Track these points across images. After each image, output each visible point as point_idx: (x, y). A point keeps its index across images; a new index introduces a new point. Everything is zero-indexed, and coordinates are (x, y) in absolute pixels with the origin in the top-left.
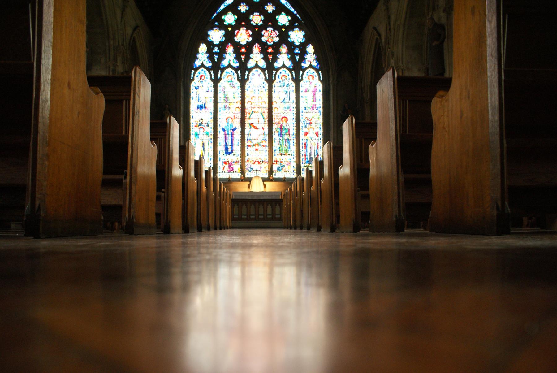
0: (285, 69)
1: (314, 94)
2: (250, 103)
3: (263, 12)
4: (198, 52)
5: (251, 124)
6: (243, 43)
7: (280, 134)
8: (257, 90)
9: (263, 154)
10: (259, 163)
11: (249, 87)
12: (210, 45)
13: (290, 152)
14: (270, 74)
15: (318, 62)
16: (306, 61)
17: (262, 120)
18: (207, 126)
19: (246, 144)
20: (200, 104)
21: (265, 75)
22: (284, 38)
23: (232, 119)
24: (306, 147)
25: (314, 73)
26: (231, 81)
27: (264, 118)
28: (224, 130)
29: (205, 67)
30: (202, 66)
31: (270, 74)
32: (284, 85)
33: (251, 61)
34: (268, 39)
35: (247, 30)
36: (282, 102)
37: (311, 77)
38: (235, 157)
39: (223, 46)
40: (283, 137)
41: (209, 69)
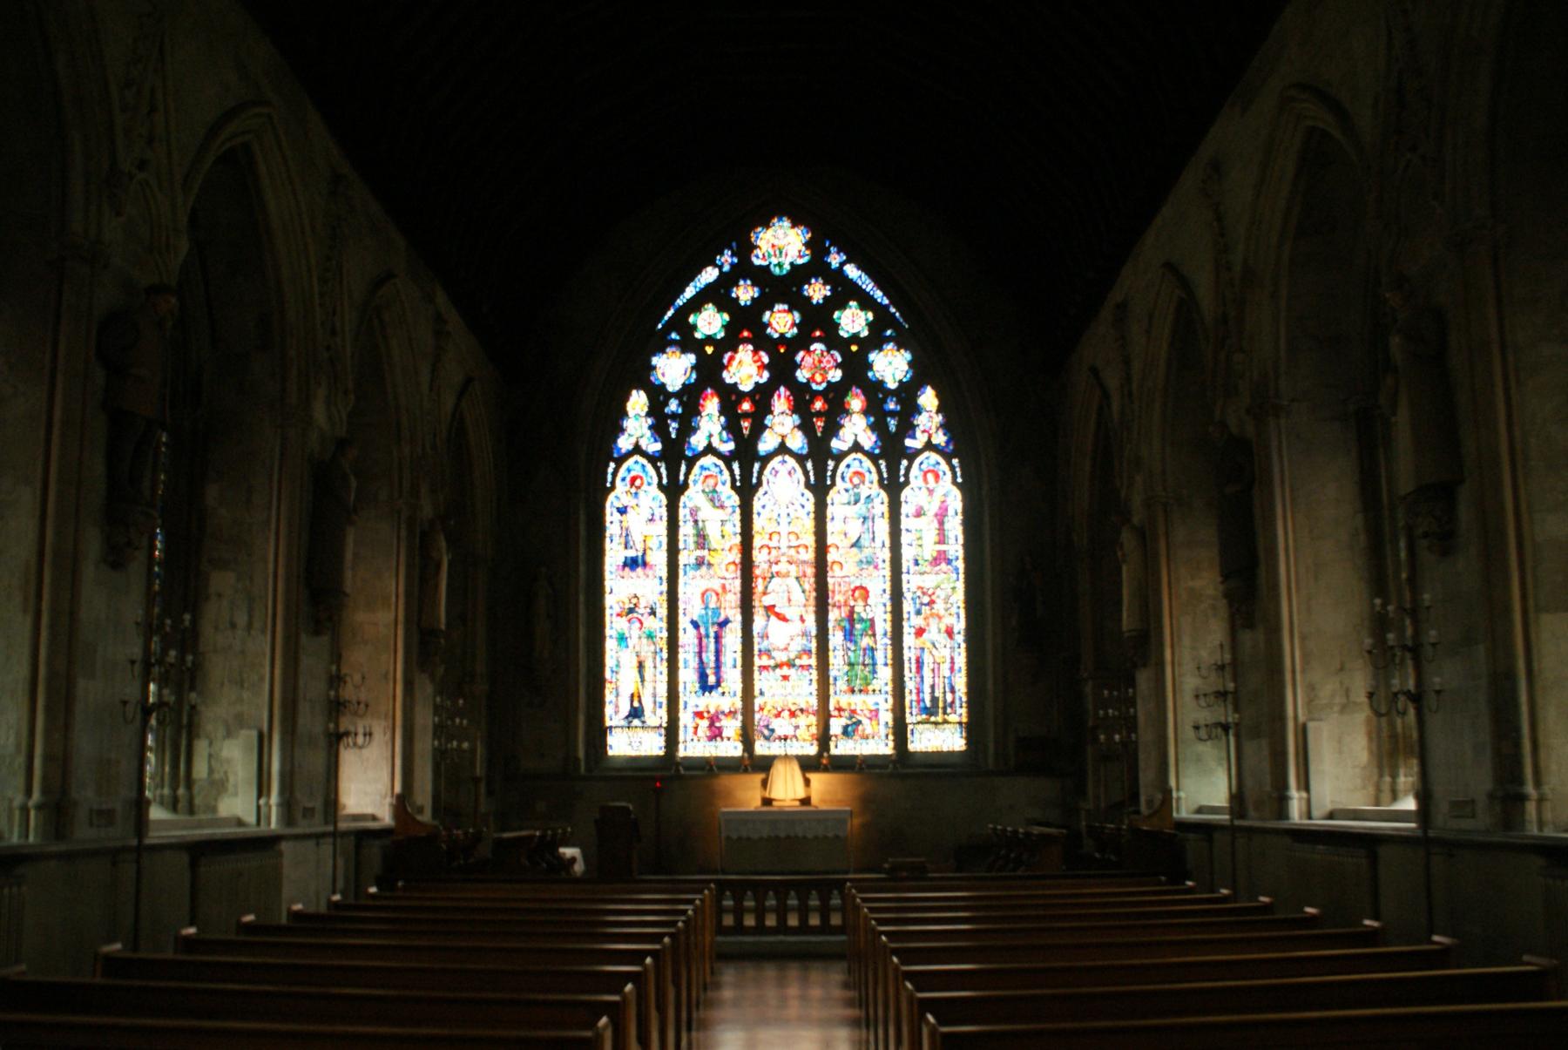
0: (860, 456)
2: (765, 551)
4: (625, 414)
6: (746, 387)
7: (849, 635)
11: (764, 507)
12: (658, 395)
13: (876, 684)
14: (820, 470)
15: (948, 435)
16: (918, 433)
17: (798, 597)
19: (757, 662)
20: (631, 553)
21: (806, 473)
23: (717, 594)
25: (938, 463)
26: (714, 491)
27: (804, 592)
28: (695, 625)
29: (644, 454)
30: (637, 450)
31: (820, 470)
33: (767, 434)
34: (813, 375)
36: (852, 546)
37: (930, 477)
38: (728, 698)
39: (691, 397)
41: (653, 459)
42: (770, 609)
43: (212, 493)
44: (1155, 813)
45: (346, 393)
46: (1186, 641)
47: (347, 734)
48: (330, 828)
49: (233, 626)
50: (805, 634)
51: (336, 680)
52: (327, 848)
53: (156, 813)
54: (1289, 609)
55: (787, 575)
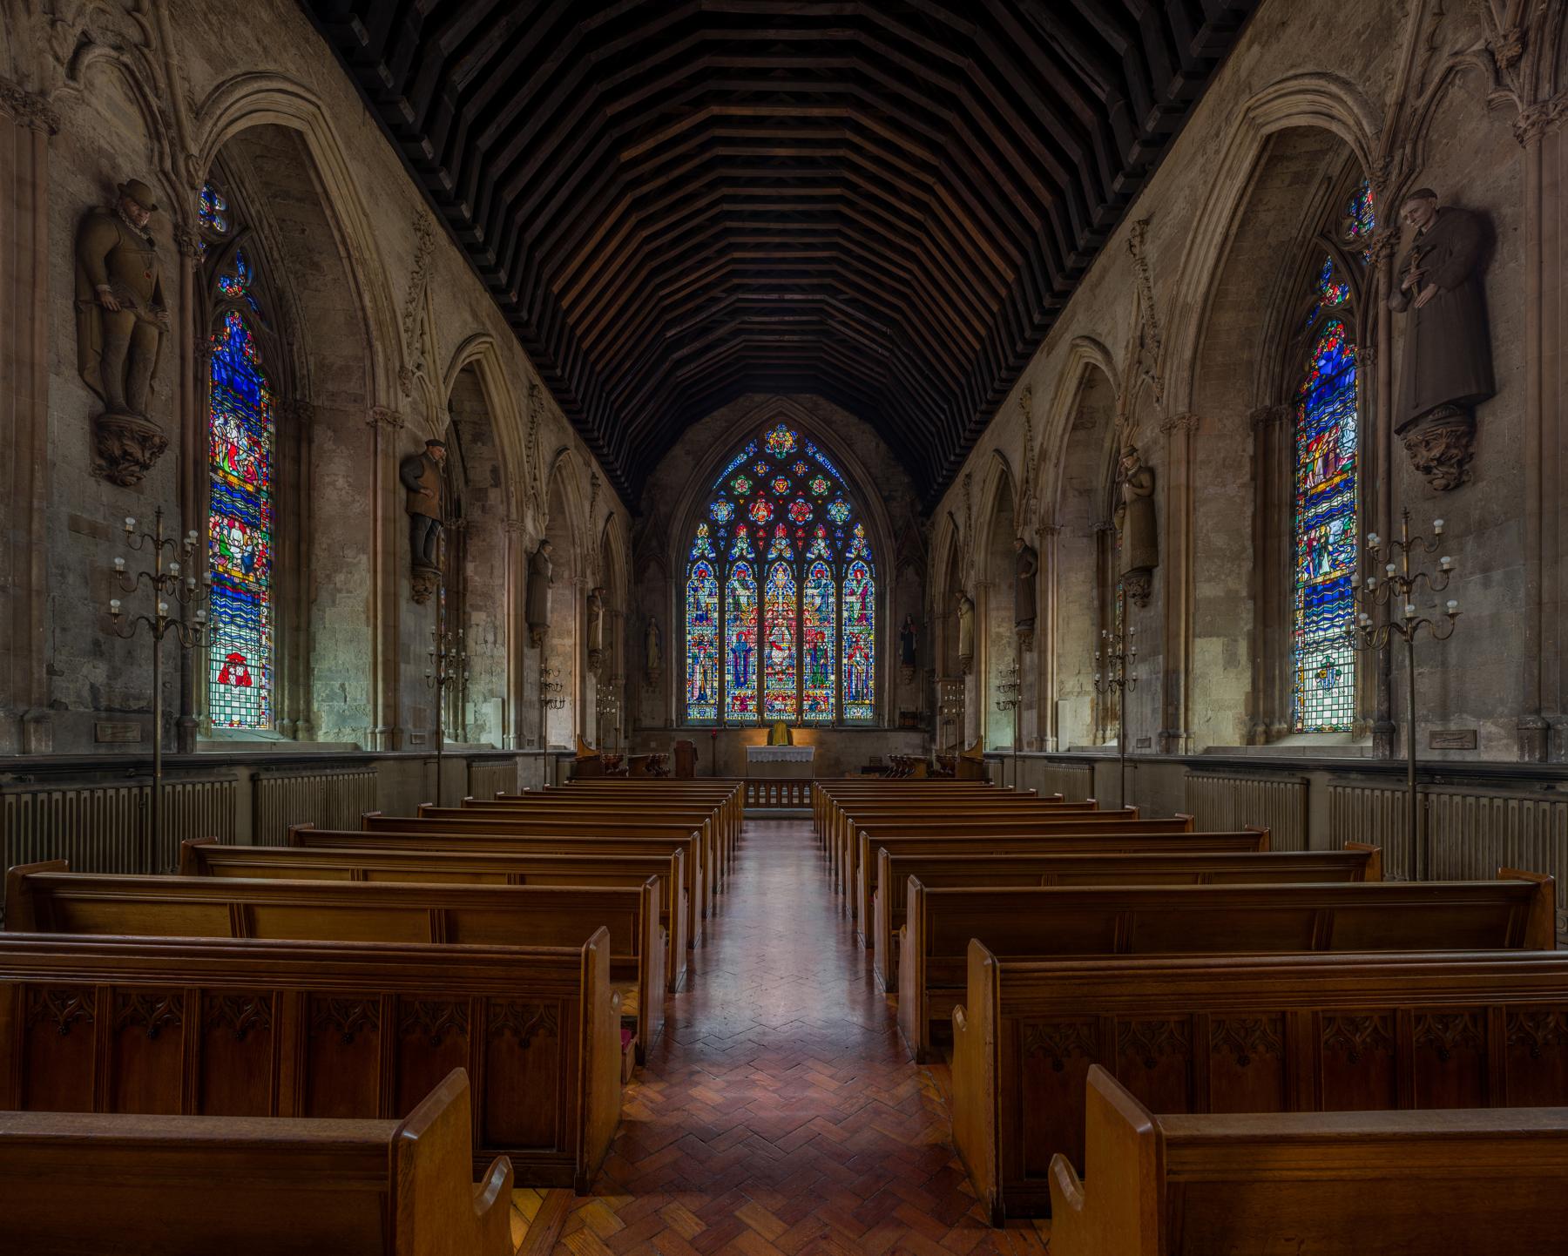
1: (864, 599)
3: (790, 475)
7: (814, 658)
9: (790, 687)
10: (784, 699)
12: (714, 526)
14: (800, 570)
17: (787, 637)
21: (792, 570)
22: (821, 513)
24: (850, 675)
27: (790, 634)
28: (734, 652)
30: (703, 557)
31: (800, 570)
35: (766, 503)
39: (732, 527)
41: (710, 561)
42: (773, 644)
43: (470, 568)
44: (972, 749)
45: (544, 514)
46: (993, 660)
47: (550, 701)
48: (543, 751)
49: (486, 642)
50: (790, 656)
51: (544, 672)
52: (541, 761)
53: (447, 741)
54: (1053, 641)
55: (782, 625)
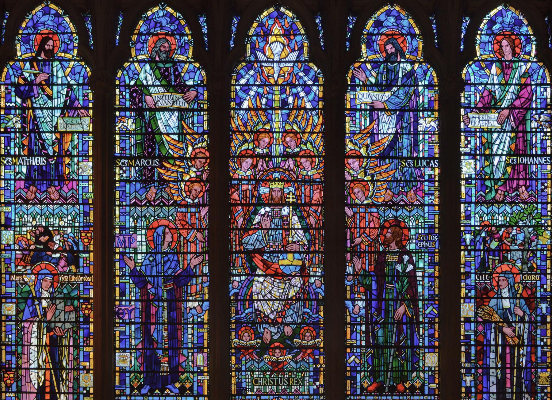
1: (522, 121)
5: (250, 255)
8: (277, 98)
11: (246, 88)
17: (299, 236)
18: (69, 264)
21: (311, 34)
24: (482, 354)
27: (306, 229)
32: (391, 76)
36: (382, 156)
40: (387, 312)
